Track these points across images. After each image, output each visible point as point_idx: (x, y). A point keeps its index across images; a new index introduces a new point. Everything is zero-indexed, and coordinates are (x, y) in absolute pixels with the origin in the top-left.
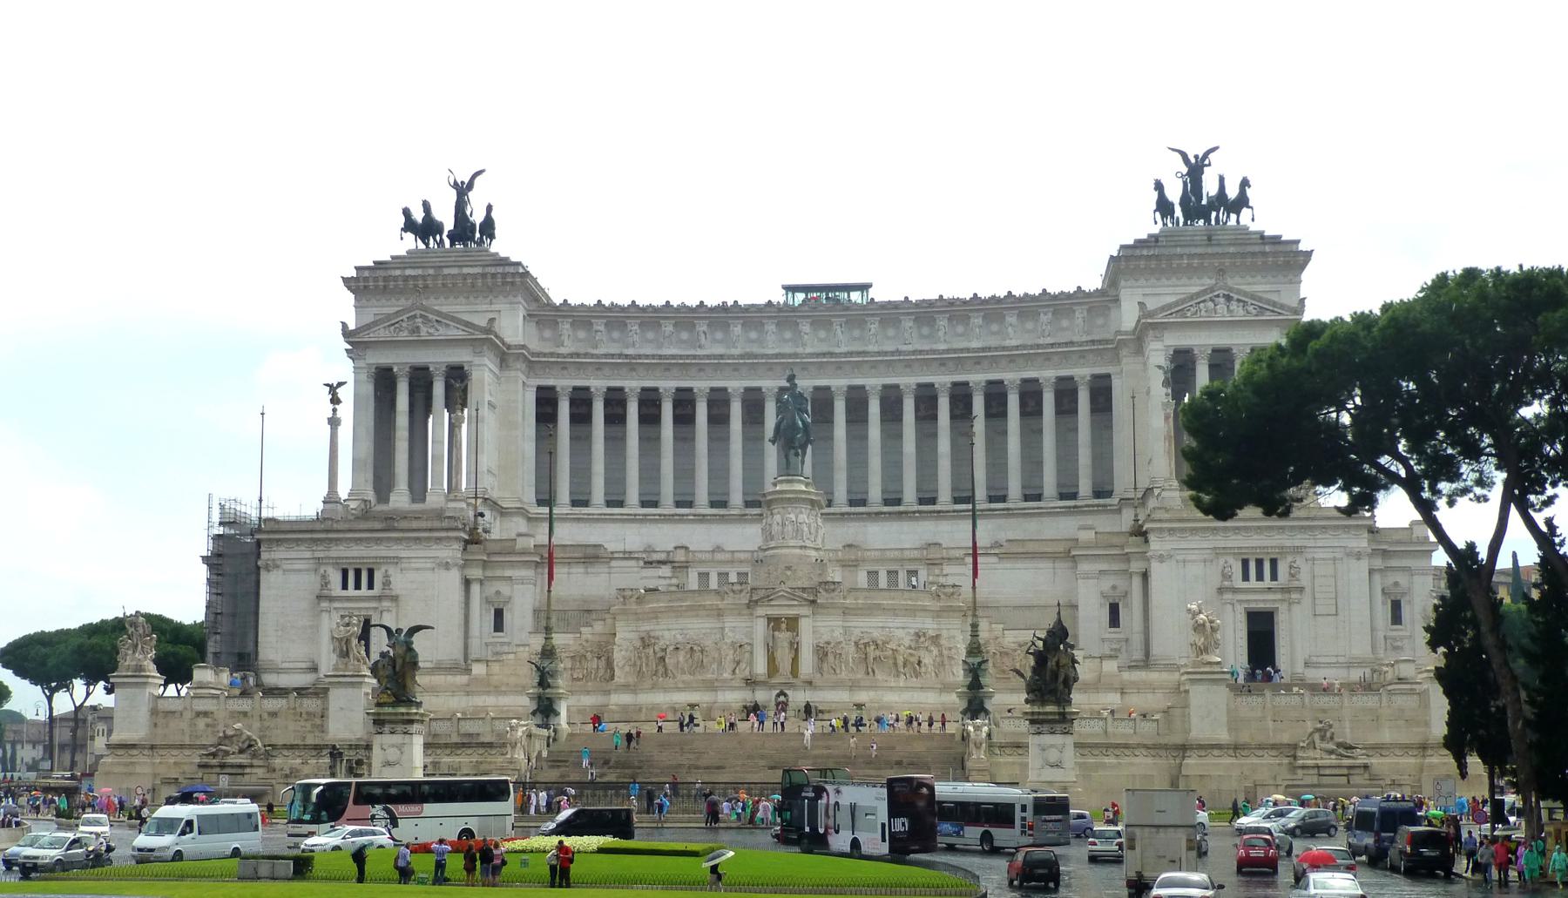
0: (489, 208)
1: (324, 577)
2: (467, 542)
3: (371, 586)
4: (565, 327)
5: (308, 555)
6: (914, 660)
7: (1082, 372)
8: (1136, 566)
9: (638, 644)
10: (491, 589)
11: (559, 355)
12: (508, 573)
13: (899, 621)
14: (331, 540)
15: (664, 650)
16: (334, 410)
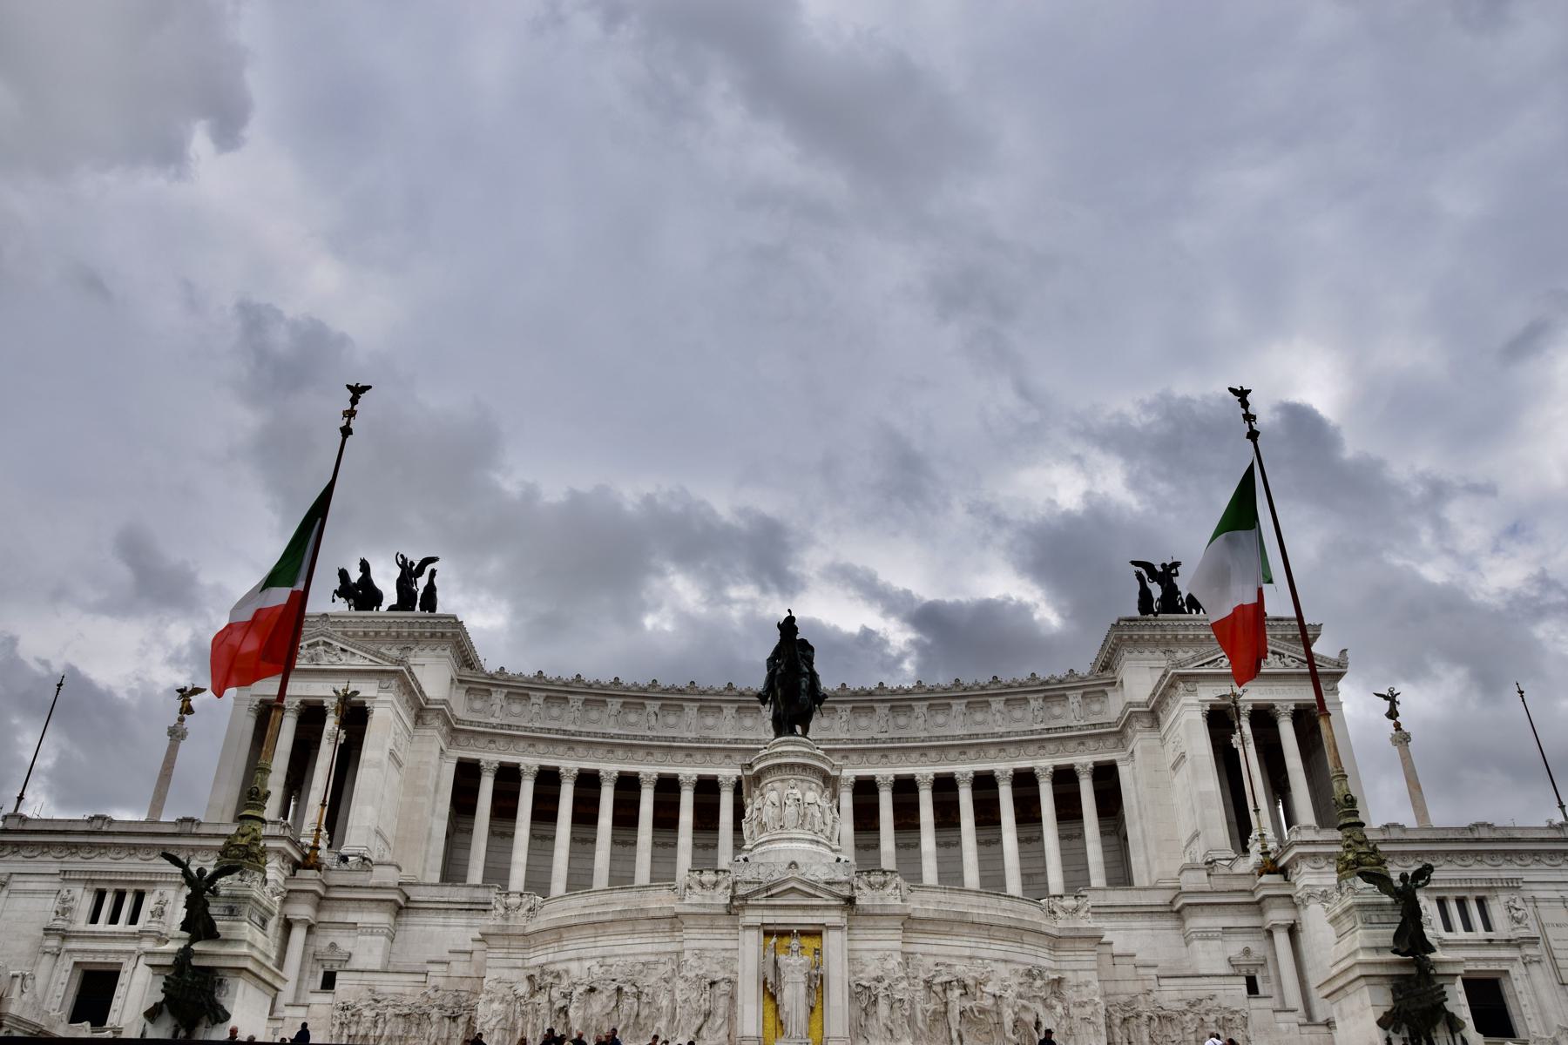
0: (433, 573)
1: (64, 901)
2: (297, 866)
3: (133, 920)
4: (498, 697)
5: (55, 868)
6: (1029, 1018)
7: (1083, 760)
8: (1278, 916)
9: (523, 988)
10: (322, 942)
11: (487, 725)
12: (352, 918)
13: (997, 949)
14: (92, 846)
15: (567, 996)
16: (181, 720)
